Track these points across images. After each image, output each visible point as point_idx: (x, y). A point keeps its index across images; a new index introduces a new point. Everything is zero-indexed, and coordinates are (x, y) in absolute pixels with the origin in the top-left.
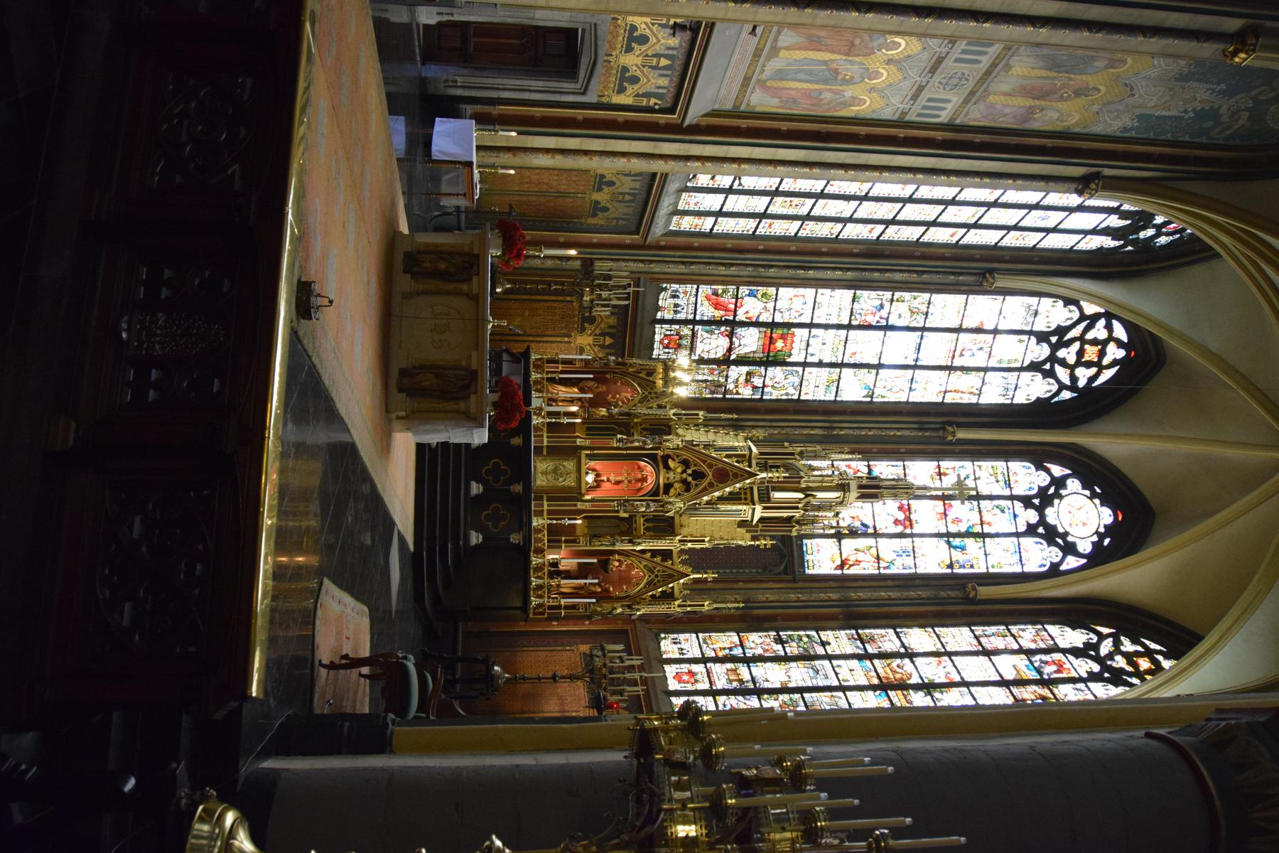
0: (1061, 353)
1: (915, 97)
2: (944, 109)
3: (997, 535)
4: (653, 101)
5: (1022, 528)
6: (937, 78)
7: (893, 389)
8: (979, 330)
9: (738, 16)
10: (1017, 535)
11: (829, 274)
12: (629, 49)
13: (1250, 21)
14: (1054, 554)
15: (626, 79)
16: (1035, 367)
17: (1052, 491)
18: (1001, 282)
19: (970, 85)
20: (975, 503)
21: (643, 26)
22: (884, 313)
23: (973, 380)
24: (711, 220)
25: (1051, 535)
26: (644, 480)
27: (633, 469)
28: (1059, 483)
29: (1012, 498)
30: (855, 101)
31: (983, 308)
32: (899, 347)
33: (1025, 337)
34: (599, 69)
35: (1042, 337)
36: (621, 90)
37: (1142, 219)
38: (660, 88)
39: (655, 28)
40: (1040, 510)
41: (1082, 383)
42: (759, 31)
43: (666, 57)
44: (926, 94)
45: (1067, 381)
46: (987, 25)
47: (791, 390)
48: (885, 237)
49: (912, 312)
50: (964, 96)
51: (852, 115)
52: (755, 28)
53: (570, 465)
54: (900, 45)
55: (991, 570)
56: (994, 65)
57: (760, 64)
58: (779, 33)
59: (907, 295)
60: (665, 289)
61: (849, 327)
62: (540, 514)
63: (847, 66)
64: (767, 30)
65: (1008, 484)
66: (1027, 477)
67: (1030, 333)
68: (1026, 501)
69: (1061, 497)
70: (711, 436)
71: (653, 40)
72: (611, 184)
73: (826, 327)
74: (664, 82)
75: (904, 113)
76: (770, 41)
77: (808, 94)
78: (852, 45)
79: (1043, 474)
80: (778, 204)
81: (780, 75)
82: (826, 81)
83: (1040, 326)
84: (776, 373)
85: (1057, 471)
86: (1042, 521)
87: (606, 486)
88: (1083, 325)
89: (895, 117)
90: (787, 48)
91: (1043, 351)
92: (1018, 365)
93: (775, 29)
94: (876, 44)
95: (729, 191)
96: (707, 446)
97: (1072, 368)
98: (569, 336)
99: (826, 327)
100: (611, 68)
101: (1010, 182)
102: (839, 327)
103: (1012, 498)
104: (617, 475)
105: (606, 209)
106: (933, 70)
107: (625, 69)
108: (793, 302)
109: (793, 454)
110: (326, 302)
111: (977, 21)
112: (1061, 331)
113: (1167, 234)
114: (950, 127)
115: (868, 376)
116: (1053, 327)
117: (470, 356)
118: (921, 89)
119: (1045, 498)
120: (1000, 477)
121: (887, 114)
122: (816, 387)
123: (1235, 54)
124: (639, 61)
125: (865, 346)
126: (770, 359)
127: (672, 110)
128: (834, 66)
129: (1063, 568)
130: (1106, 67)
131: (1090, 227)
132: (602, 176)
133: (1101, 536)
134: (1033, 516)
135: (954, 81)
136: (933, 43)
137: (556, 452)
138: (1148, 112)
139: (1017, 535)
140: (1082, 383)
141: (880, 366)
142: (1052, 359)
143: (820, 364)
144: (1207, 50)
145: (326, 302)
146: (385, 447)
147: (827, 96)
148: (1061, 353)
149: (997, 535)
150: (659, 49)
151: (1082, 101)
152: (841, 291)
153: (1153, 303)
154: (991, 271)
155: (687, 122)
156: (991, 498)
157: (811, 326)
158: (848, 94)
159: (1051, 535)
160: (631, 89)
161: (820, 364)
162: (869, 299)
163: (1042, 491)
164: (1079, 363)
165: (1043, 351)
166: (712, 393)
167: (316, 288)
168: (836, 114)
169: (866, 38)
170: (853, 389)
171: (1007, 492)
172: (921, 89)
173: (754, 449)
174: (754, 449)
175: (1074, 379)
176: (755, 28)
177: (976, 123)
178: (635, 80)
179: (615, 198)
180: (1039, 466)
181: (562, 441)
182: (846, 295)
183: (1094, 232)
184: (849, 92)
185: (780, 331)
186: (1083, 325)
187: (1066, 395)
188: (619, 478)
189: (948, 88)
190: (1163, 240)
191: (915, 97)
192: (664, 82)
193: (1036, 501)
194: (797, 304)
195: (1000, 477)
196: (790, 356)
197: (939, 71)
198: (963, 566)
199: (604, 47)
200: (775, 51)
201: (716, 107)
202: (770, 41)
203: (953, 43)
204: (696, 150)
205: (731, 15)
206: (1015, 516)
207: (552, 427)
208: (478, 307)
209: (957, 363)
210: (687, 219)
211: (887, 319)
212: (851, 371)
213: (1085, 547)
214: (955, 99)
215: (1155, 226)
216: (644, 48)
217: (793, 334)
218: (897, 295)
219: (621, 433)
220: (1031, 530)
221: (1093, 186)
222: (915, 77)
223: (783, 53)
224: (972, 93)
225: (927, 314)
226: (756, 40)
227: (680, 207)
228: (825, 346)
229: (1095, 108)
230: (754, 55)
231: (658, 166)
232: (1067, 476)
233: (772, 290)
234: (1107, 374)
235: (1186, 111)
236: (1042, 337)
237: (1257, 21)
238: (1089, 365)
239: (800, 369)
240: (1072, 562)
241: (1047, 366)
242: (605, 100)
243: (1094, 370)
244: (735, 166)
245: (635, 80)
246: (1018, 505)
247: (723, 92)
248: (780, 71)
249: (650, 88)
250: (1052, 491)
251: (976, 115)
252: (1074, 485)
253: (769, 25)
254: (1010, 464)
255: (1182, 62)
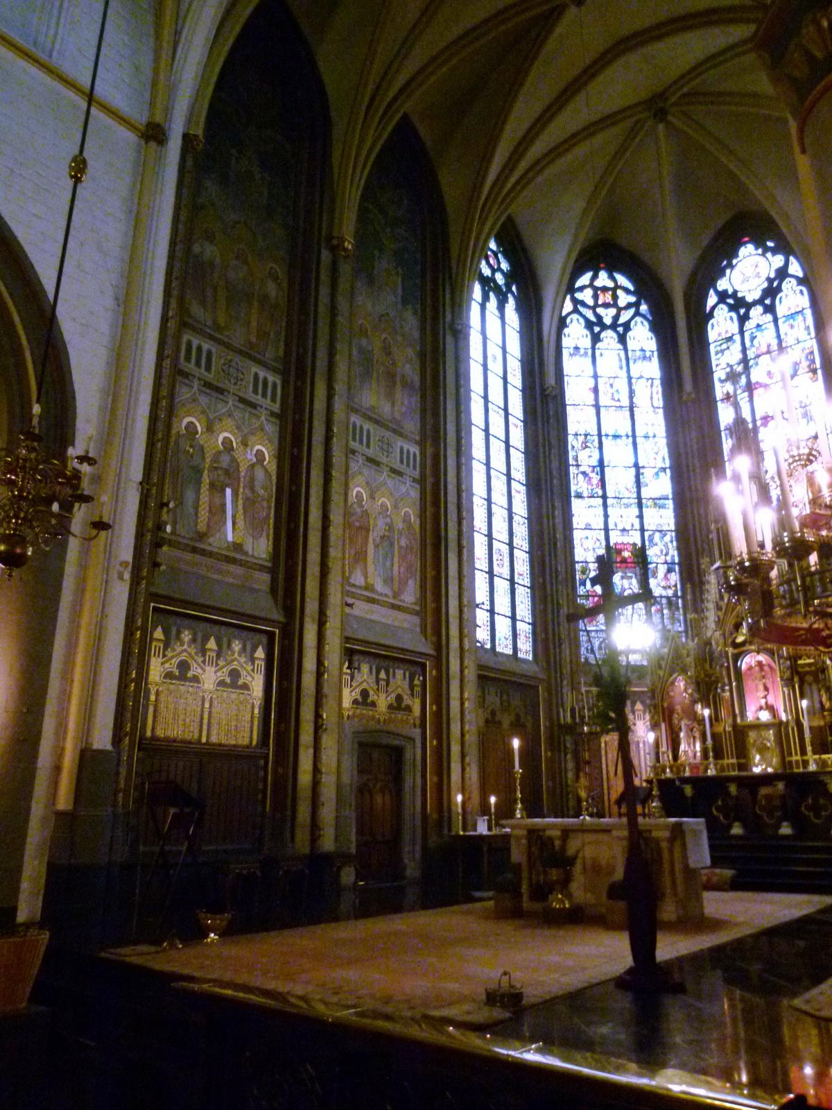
0: (608, 321)
1: (400, 474)
2: (408, 451)
3: (779, 336)
4: (416, 682)
5: (769, 317)
6: (384, 460)
7: (656, 452)
8: (596, 390)
9: (338, 620)
10: (776, 320)
11: (559, 520)
12: (373, 704)
13: (323, 245)
14: (789, 286)
15: (398, 705)
16: (622, 339)
17: (731, 301)
18: (551, 380)
19: (388, 434)
20: (751, 363)
21: (353, 694)
22: (589, 470)
23: (639, 387)
24: (519, 625)
25: (772, 292)
26: (760, 664)
27: (752, 675)
28: (723, 296)
29: (742, 332)
30: (406, 519)
31: (576, 390)
32: (618, 455)
33: (598, 353)
34: (391, 728)
35: (596, 339)
36: (409, 709)
37: (487, 283)
38: (405, 677)
39: (354, 684)
40: (749, 306)
41: (632, 299)
42: (350, 601)
43: (378, 672)
44: (397, 466)
45: (632, 311)
46: (335, 430)
47: (667, 538)
48: (523, 479)
49: (587, 447)
50: (397, 437)
51: (418, 521)
52: (347, 605)
53: (752, 735)
54: (358, 492)
55: (813, 334)
56: (370, 419)
57: (380, 598)
58: (354, 585)
59: (571, 454)
60: (586, 659)
61: (604, 497)
62: (806, 763)
63: (378, 527)
64: (349, 594)
65: (730, 339)
66: (722, 323)
67: (593, 348)
68: (743, 319)
69: (735, 292)
70: (711, 606)
71: (364, 686)
72: (493, 713)
73: (606, 516)
74: (399, 673)
75: (414, 480)
76: (359, 592)
77: (403, 557)
78: (360, 528)
79: (716, 313)
80: (501, 570)
81: (388, 580)
82: (392, 544)
83: (586, 342)
84: (652, 553)
85: (712, 299)
86: (760, 301)
87: (771, 700)
88: (581, 309)
89: (418, 486)
90: (366, 578)
91: (609, 337)
92: (622, 354)
93: (348, 588)
94: (359, 510)
95: (492, 611)
96: (719, 608)
97: (620, 310)
98: (638, 743)
99: (606, 516)
100: (390, 718)
101: (462, 390)
102: (605, 506)
103: (742, 332)
104: (757, 690)
105: (518, 716)
106: (378, 464)
107: (390, 707)
108: (587, 549)
109: (718, 529)
110: (505, 979)
111: (332, 437)
112: (589, 325)
113: (499, 263)
114: (422, 443)
115: (647, 475)
116: (586, 332)
117: (618, 837)
118: (393, 471)
119: (739, 306)
120: (724, 346)
121: (415, 494)
122: (663, 518)
123: (345, 250)
124: (383, 696)
125: (619, 480)
126: (640, 560)
127: (423, 666)
128: (378, 539)
129: (801, 274)
130: (367, 336)
131: (499, 322)
132: (487, 721)
133: (766, 250)
134: (756, 312)
135: (385, 447)
136: (354, 466)
137: (742, 751)
138: (399, 299)
139: (776, 320)
140: (632, 299)
141: (636, 465)
142: (614, 326)
143: (641, 517)
144: (345, 268)
145: (505, 979)
146: (715, 925)
147: (403, 542)
148: (608, 321)
149: (779, 336)
150: (372, 680)
151: (394, 349)
152: (573, 508)
153: (553, 259)
154: (543, 390)
155: (432, 652)
156: (744, 350)
157: (606, 530)
158: (401, 525)
159: (772, 292)
160: (407, 700)
161: (641, 517)
162: (578, 484)
163: (732, 308)
164: (615, 305)
165: (609, 337)
166: (678, 608)
167: (493, 986)
168: (418, 530)
169: (353, 518)
170: (661, 485)
171: (737, 338)
172: (393, 471)
173: (717, 564)
174: (717, 564)
175: (629, 306)
176: (347, 605)
177: (418, 424)
178: (399, 698)
179: (505, 708)
180: (711, 315)
181: (728, 745)
182: (576, 505)
183: (502, 317)
184: (400, 525)
185: (614, 556)
186: (581, 309)
187: (644, 308)
188: (761, 687)
189: (391, 450)
190: (505, 266)
191: (400, 474)
192: (399, 673)
193: (742, 311)
194: (589, 544)
195: (724, 346)
196: (635, 545)
197: (378, 459)
198: (813, 361)
199: (372, 725)
200: (369, 587)
201: (418, 629)
202: (359, 592)
203: (353, 452)
204: (454, 643)
205: (338, 625)
206: (758, 326)
207: (718, 755)
208: (573, 831)
209: (626, 402)
210: (520, 645)
211: (594, 467)
212: (643, 490)
213: (778, 261)
214: (399, 444)
215: (493, 274)
216: (371, 693)
217: (616, 544)
218: (571, 461)
219: (716, 688)
220: (770, 309)
221: (460, 327)
222: (384, 476)
223: (370, 581)
224: (394, 431)
225: (586, 435)
226: (357, 603)
227: (510, 652)
228: (623, 516)
229: (399, 338)
230: (373, 603)
231: (471, 674)
232: (717, 292)
233: (578, 567)
234: (622, 280)
235: (397, 274)
236: (596, 339)
237: (323, 239)
238: (615, 297)
239: (647, 534)
240: (795, 268)
241: (620, 329)
242: (418, 722)
243: (619, 292)
244: (466, 609)
245: (399, 698)
246: (749, 325)
247: (406, 625)
248: (385, 581)
249: (406, 685)
250: (731, 301)
251: (412, 426)
252: (722, 284)
253: (346, 593)
254: (711, 341)
255: (359, 284)
